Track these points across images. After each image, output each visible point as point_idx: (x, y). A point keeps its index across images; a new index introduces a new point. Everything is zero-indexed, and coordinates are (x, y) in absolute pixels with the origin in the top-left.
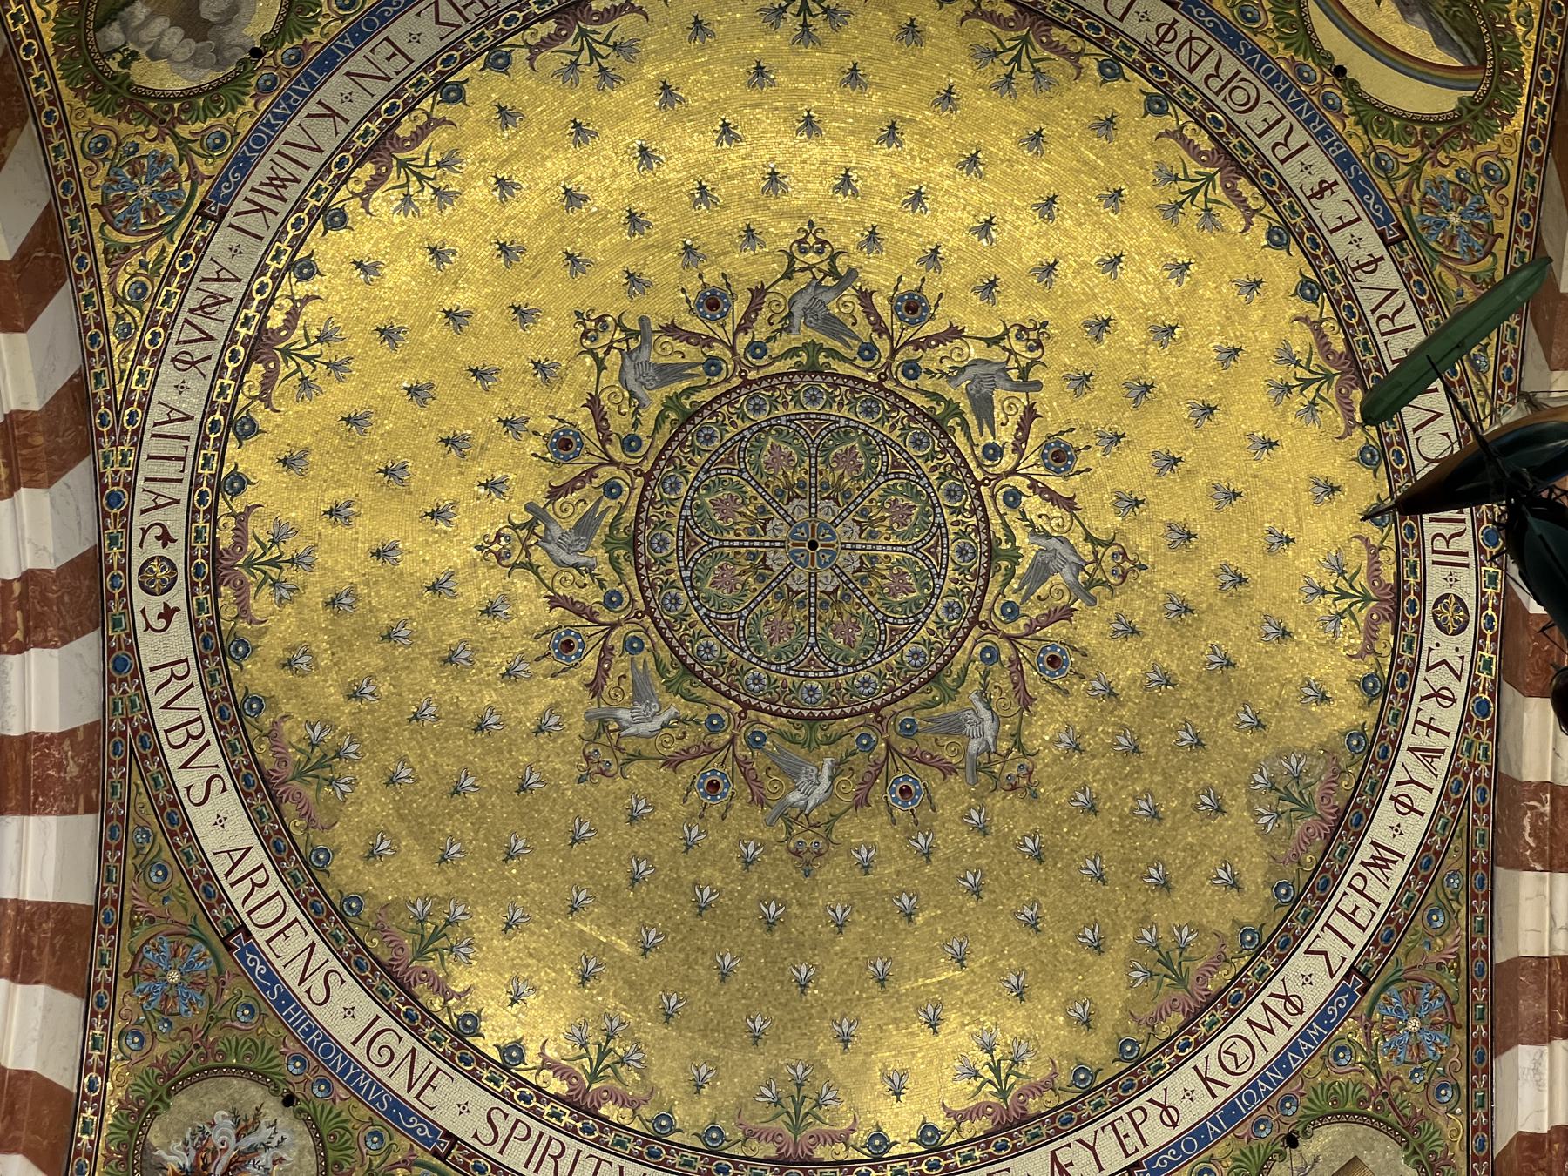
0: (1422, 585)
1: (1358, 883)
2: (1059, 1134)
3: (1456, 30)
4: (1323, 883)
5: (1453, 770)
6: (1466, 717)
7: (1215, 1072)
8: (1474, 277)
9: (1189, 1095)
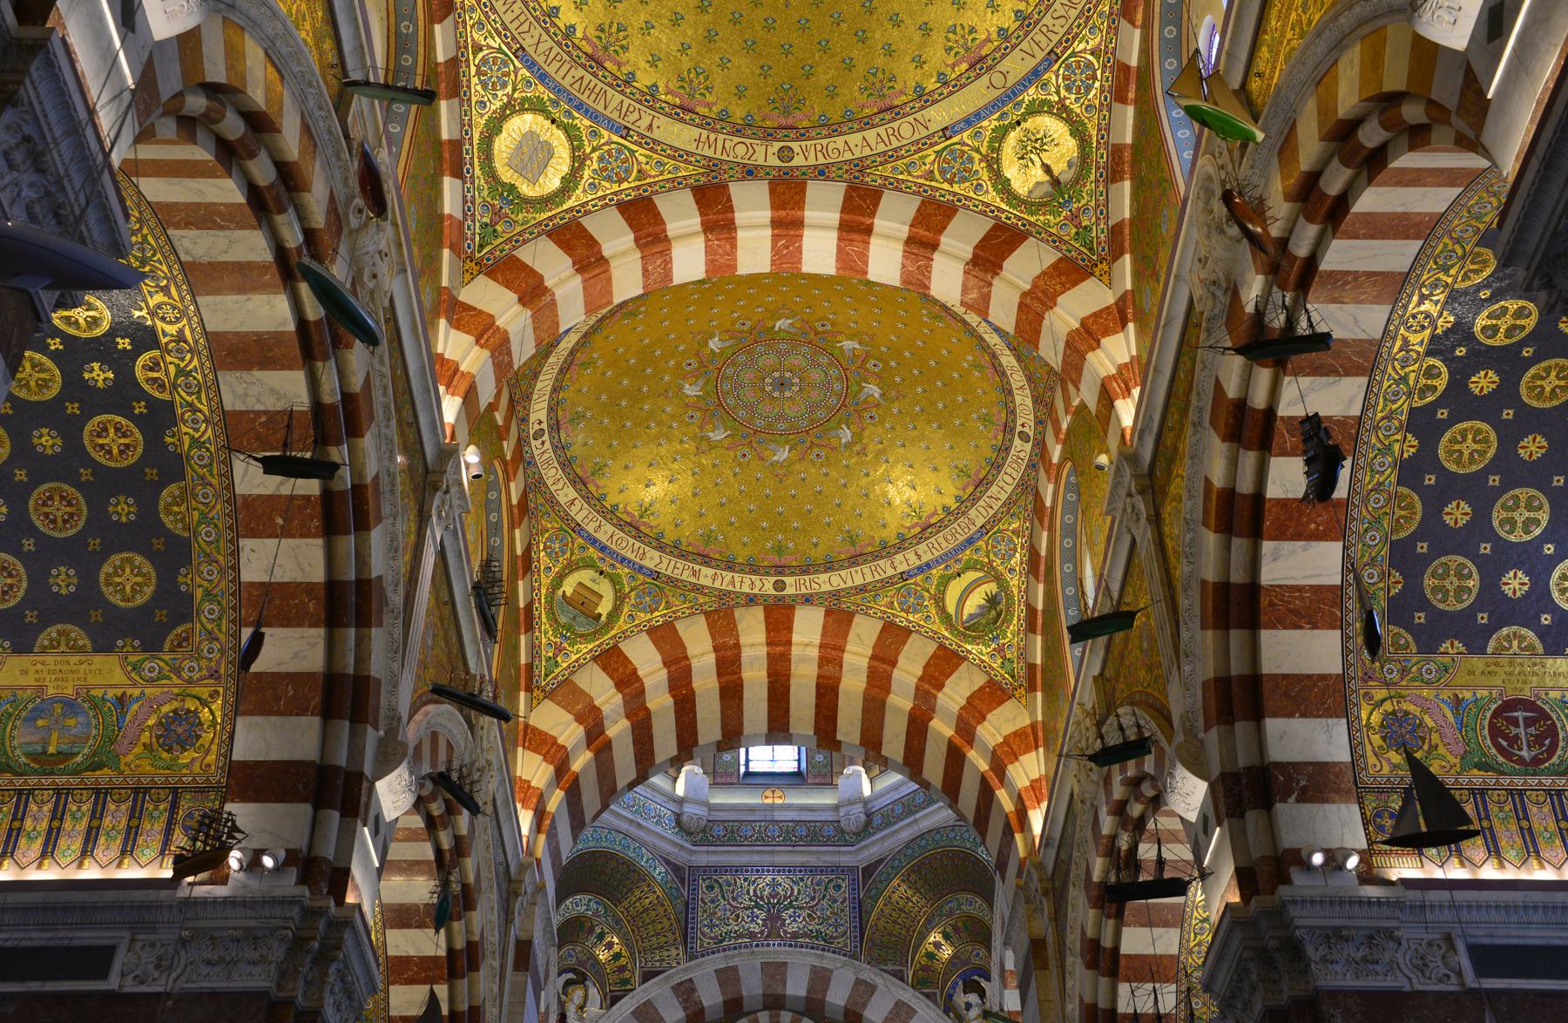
2: (583, 497)
4: (683, 556)
5: (729, 592)
6: (748, 595)
7: (615, 538)
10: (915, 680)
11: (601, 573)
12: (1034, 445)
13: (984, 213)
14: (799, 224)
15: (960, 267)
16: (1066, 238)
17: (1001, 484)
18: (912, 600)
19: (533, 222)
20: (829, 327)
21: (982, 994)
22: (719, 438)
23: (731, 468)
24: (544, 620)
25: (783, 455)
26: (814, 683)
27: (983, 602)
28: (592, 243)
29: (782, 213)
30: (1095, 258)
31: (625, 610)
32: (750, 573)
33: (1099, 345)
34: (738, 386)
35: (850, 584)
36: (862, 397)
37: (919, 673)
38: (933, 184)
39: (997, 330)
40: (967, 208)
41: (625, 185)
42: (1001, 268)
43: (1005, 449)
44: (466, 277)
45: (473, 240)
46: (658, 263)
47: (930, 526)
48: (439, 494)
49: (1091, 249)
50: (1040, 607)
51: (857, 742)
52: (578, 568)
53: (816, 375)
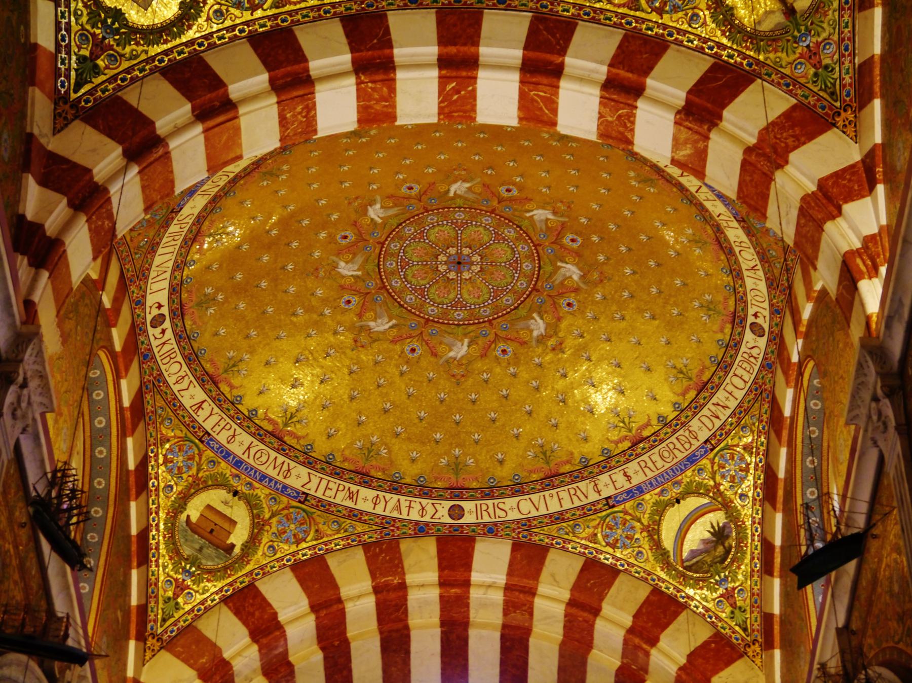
0: (466, 500)
1: (341, 488)
2: (213, 399)
3: (697, 562)
4: (337, 473)
5: (394, 519)
6: (417, 523)
7: (253, 451)
8: (596, 535)
9: (241, 443)
11: (235, 493)
12: (769, 340)
13: (700, 50)
14: (472, 63)
15: (670, 117)
16: (803, 81)
17: (730, 388)
18: (619, 531)
19: (143, 57)
20: (515, 192)
22: (382, 328)
23: (397, 366)
24: (163, 551)
25: (461, 350)
26: (497, 635)
27: (707, 535)
28: (218, 84)
29: (452, 50)
30: (838, 104)
31: (265, 540)
32: (420, 496)
33: (840, 213)
34: (405, 264)
35: (542, 511)
36: (558, 278)
37: (628, 621)
38: (638, 14)
39: (720, 196)
40: (679, 43)
41: (259, 13)
42: (720, 118)
43: (734, 345)
44: (60, 123)
45: (68, 77)
46: (299, 109)
47: (643, 440)
48: (13, 389)
49: (832, 94)
50: (778, 542)
52: (206, 487)
53: (502, 252)
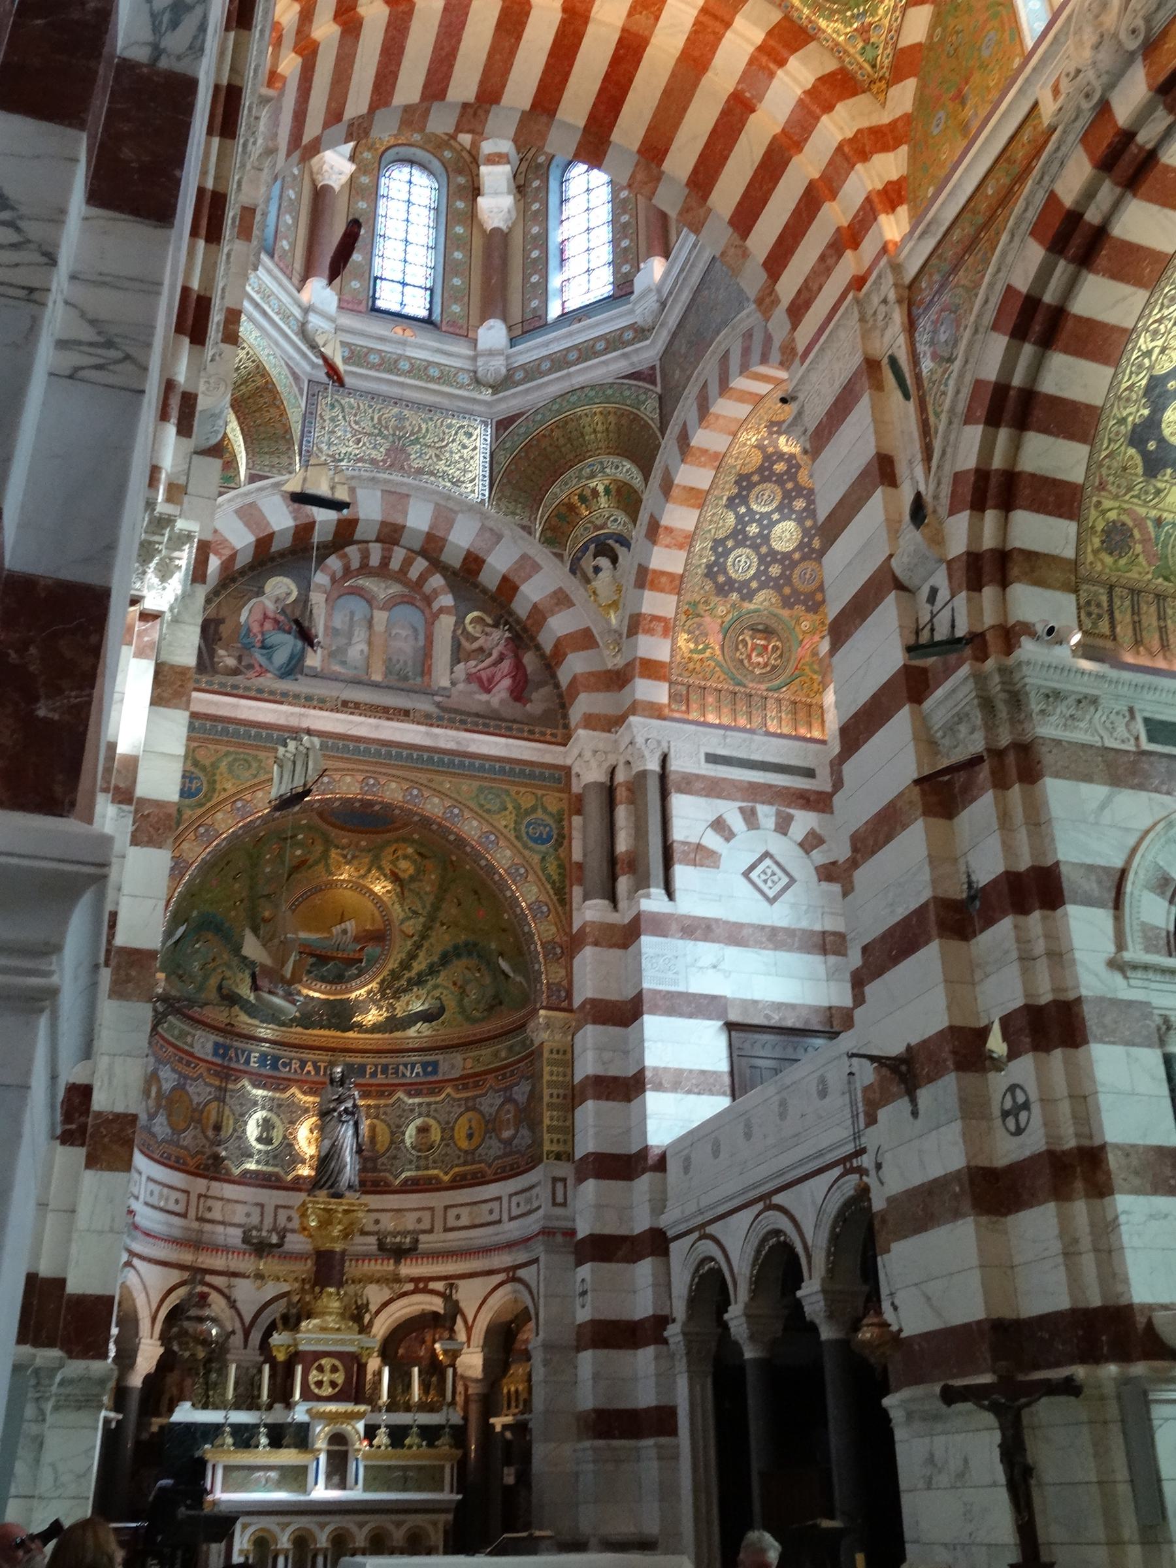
10: (751, 49)
21: (614, 560)
26: (616, 37)
51: (636, 146)
